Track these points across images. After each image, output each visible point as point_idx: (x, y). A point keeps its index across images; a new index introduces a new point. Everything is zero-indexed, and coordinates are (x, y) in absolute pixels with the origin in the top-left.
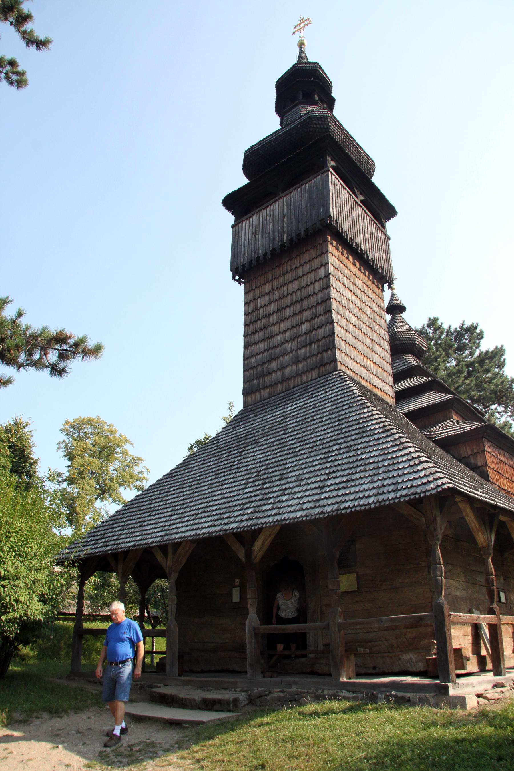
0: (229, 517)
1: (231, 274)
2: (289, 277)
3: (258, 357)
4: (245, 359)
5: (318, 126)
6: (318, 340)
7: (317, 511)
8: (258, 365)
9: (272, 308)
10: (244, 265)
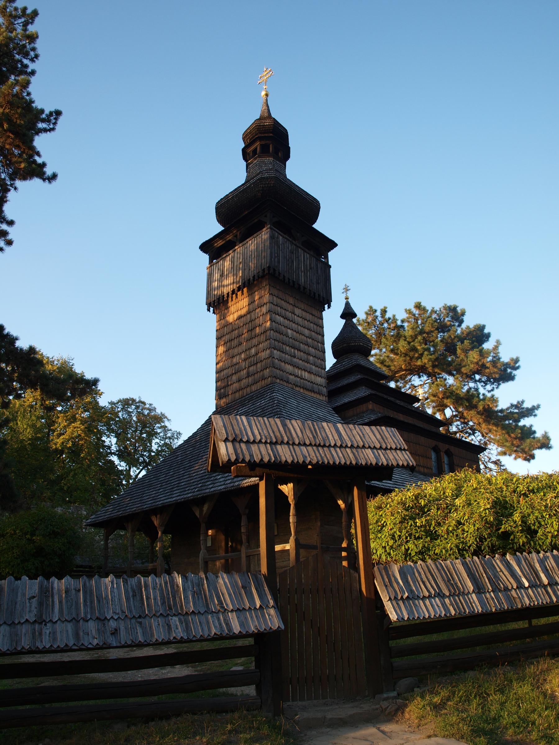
0: (189, 490)
1: (206, 307)
3: (225, 371)
4: (217, 372)
5: (266, 186)
6: (261, 361)
7: (232, 485)
10: (214, 301)
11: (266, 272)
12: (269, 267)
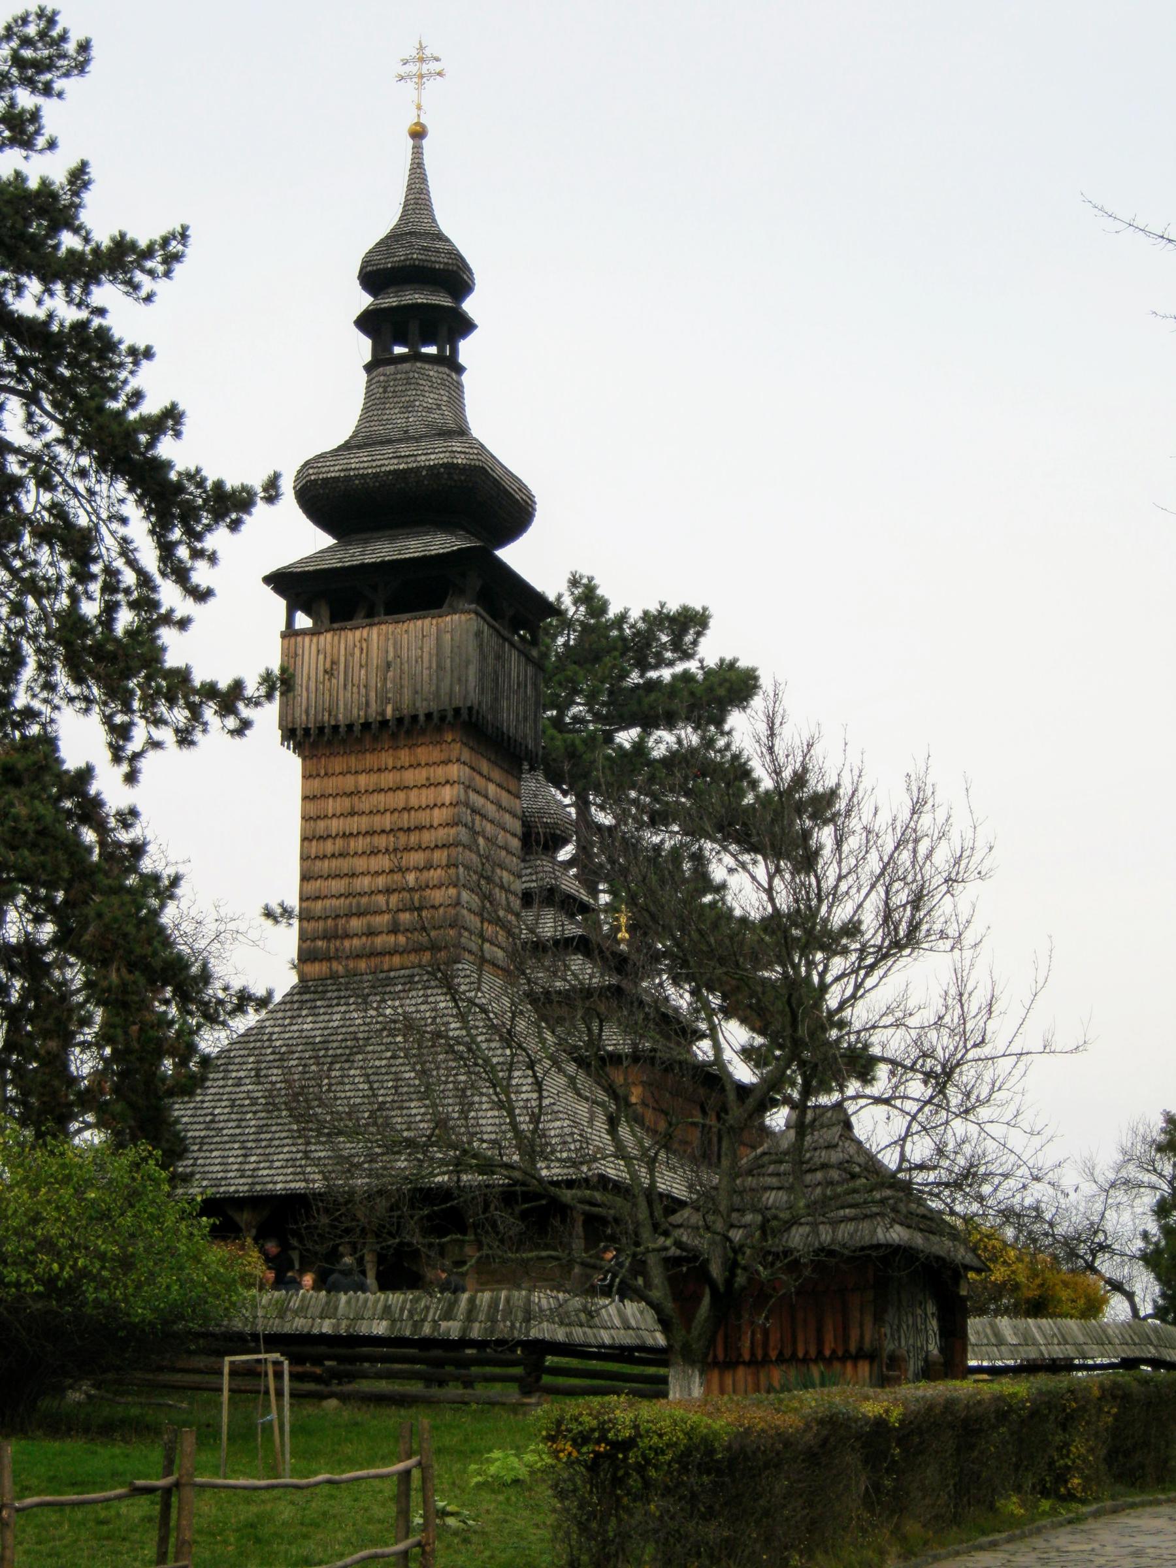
2: (388, 779)
8: (327, 917)
9: (354, 824)
11: (465, 714)
12: (470, 709)
